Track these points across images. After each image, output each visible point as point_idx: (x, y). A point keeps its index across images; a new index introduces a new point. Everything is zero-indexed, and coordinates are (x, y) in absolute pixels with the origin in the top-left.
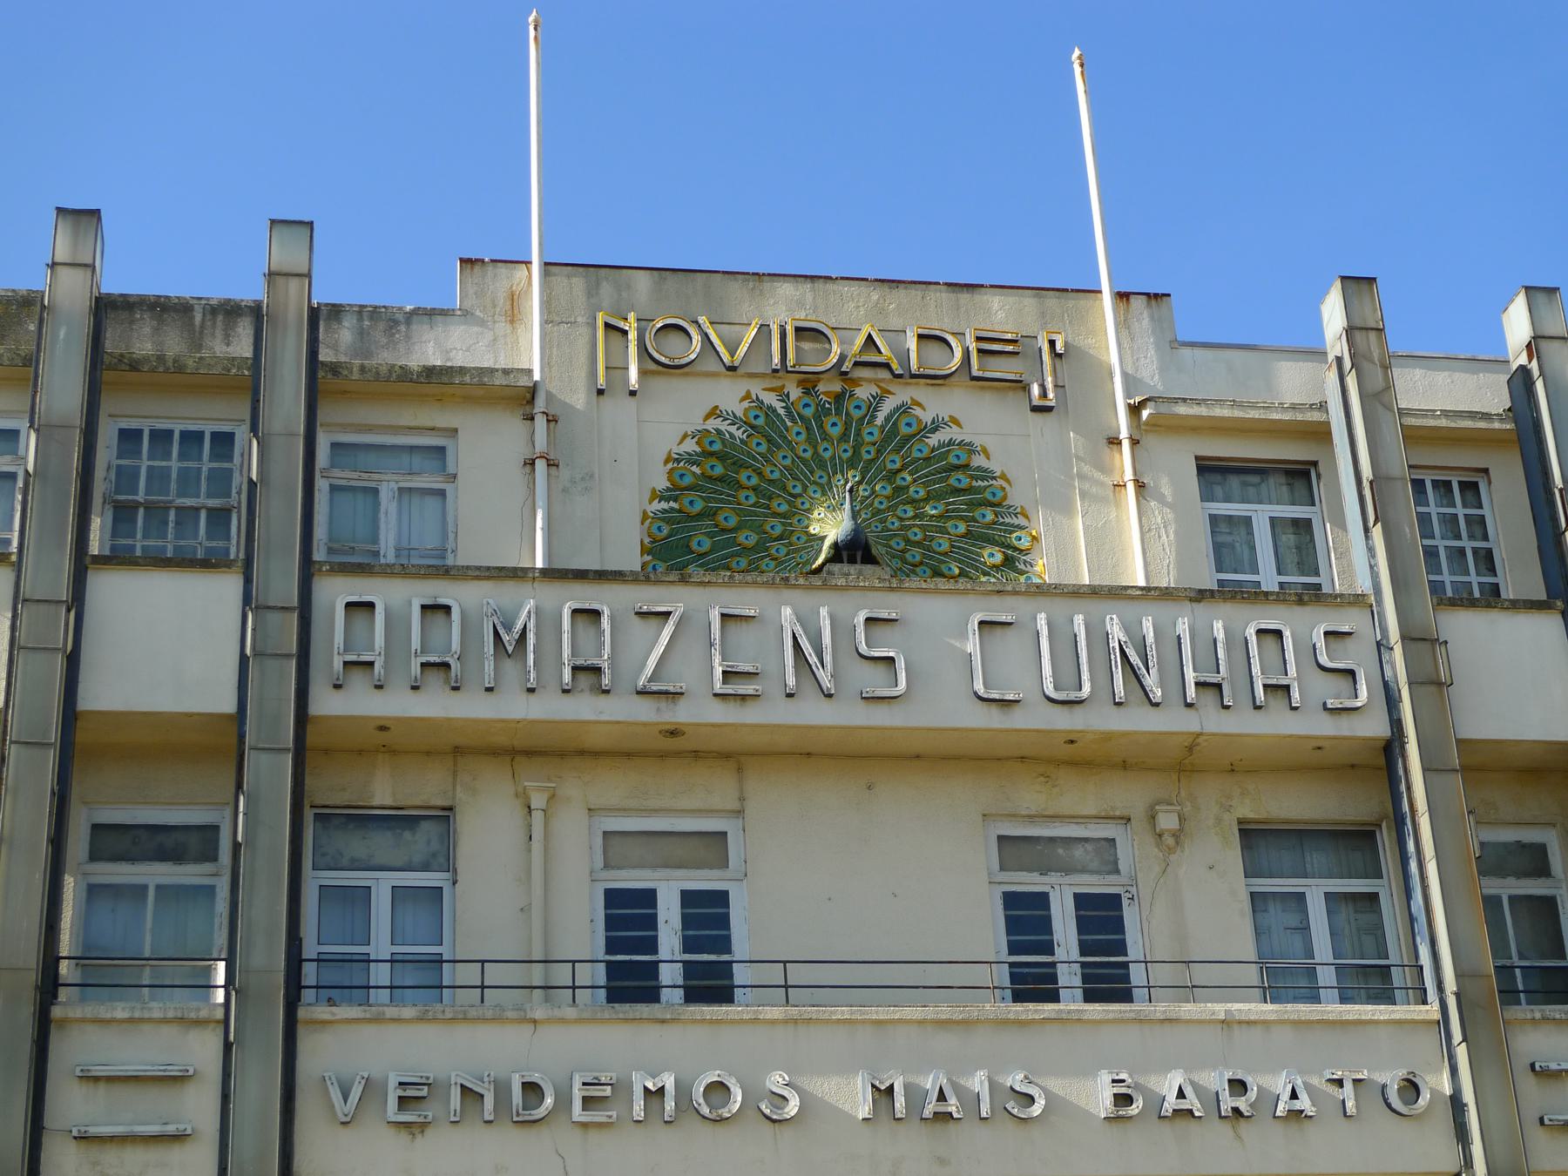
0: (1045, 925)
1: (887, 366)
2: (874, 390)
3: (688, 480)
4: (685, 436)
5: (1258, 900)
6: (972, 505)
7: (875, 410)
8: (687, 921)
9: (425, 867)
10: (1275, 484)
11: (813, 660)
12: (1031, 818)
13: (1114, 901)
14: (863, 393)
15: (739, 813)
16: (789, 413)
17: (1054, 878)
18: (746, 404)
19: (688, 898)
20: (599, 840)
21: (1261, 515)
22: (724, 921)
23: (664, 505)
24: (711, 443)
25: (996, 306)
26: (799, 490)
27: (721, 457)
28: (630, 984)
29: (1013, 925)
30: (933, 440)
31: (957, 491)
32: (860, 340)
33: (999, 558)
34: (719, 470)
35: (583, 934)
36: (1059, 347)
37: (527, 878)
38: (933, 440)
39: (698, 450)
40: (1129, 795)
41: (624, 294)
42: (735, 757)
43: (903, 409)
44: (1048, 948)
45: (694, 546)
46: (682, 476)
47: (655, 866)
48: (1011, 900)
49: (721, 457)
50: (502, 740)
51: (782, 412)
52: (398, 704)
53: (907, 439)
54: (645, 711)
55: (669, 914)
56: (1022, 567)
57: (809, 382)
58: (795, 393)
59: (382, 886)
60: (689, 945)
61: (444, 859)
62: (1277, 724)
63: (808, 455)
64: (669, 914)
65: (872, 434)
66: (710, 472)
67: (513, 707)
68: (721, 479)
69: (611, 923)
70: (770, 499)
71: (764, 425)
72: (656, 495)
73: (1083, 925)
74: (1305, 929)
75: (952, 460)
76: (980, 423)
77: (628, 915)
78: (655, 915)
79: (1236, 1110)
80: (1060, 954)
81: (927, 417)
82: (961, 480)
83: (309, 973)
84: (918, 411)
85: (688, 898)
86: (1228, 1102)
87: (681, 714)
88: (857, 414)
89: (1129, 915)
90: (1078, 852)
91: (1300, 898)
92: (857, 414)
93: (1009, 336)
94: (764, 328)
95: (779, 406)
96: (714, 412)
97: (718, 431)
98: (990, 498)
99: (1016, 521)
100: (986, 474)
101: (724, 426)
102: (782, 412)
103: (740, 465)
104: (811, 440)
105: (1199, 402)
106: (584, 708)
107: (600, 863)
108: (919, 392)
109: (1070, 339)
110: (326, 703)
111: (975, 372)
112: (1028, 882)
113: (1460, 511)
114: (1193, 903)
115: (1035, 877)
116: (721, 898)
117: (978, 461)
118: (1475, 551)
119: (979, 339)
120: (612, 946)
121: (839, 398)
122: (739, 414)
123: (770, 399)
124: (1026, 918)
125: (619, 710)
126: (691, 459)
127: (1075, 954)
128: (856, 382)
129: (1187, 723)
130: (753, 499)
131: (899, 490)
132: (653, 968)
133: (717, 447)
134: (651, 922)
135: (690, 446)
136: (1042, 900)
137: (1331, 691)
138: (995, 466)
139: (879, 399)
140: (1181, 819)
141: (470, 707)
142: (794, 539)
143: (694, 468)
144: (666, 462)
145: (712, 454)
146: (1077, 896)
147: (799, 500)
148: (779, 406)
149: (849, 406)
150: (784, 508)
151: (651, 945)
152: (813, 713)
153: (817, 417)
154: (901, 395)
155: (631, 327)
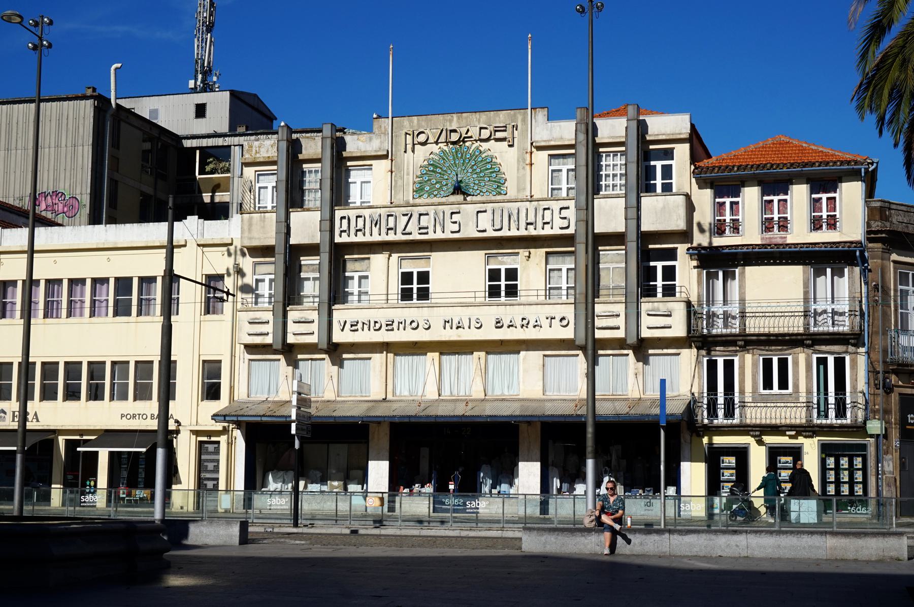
14: (467, 144)
31: (487, 169)
32: (464, 130)
35: (396, 286)
52: (353, 239)
57: (454, 143)
62: (548, 231)
67: (376, 238)
71: (443, 155)
72: (417, 177)
76: (496, 149)
77: (406, 278)
82: (489, 166)
91: (560, 270)
100: (496, 164)
103: (437, 167)
104: (454, 159)
106: (391, 237)
108: (482, 144)
117: (494, 160)
123: (446, 148)
125: (400, 237)
131: (474, 170)
135: (426, 163)
138: (498, 161)
141: (367, 239)
152: (440, 235)
153: (456, 152)
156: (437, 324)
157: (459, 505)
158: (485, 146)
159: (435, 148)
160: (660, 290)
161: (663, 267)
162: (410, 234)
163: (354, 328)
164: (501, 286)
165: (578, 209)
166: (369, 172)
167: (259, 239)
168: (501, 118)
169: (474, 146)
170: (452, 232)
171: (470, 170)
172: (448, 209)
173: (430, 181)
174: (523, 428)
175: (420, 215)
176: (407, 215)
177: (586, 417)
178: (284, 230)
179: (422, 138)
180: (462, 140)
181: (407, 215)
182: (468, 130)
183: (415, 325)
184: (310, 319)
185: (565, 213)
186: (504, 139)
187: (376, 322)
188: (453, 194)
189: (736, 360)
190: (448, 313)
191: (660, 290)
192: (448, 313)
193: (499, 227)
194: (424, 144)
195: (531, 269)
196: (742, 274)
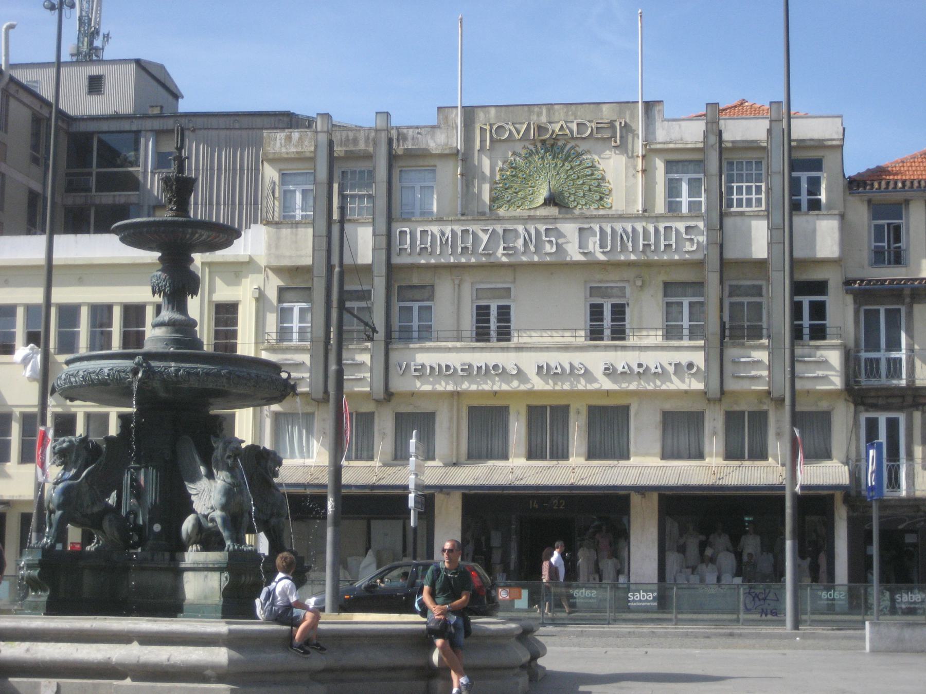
0: (602, 313)
2: (564, 142)
5: (668, 304)
8: (499, 314)
9: (428, 300)
10: (691, 167)
12: (600, 282)
13: (623, 306)
14: (560, 143)
15: (514, 282)
19: (499, 307)
20: (475, 292)
21: (685, 177)
22: (509, 314)
27: (515, 168)
28: (482, 335)
29: (592, 313)
32: (557, 127)
35: (468, 321)
37: (451, 305)
40: (629, 274)
42: (513, 267)
43: (573, 148)
44: (602, 320)
47: (490, 299)
48: (592, 306)
49: (515, 168)
55: (494, 312)
59: (416, 306)
60: (499, 321)
61: (431, 298)
64: (494, 312)
68: (514, 176)
69: (478, 315)
73: (613, 313)
74: (682, 312)
77: (482, 313)
79: (639, 372)
81: (579, 150)
83: (395, 335)
84: (577, 149)
85: (499, 307)
86: (636, 369)
88: (557, 151)
89: (627, 310)
91: (682, 303)
92: (557, 151)
94: (529, 125)
107: (475, 297)
108: (579, 143)
109: (628, 121)
112: (598, 301)
114: (647, 308)
116: (508, 307)
120: (478, 321)
121: (552, 146)
124: (596, 312)
128: (558, 140)
134: (489, 314)
139: (565, 145)
140: (643, 281)
149: (555, 148)
151: (488, 321)
155: (488, 127)
157: (591, 598)
158: (582, 147)
160: (806, 331)
161: (811, 303)
165: (709, 228)
167: (291, 257)
174: (635, 499)
177: (782, 488)
178: (324, 247)
187: (448, 367)
189: (902, 418)
190: (544, 358)
191: (806, 331)
192: (544, 358)
196: (910, 314)
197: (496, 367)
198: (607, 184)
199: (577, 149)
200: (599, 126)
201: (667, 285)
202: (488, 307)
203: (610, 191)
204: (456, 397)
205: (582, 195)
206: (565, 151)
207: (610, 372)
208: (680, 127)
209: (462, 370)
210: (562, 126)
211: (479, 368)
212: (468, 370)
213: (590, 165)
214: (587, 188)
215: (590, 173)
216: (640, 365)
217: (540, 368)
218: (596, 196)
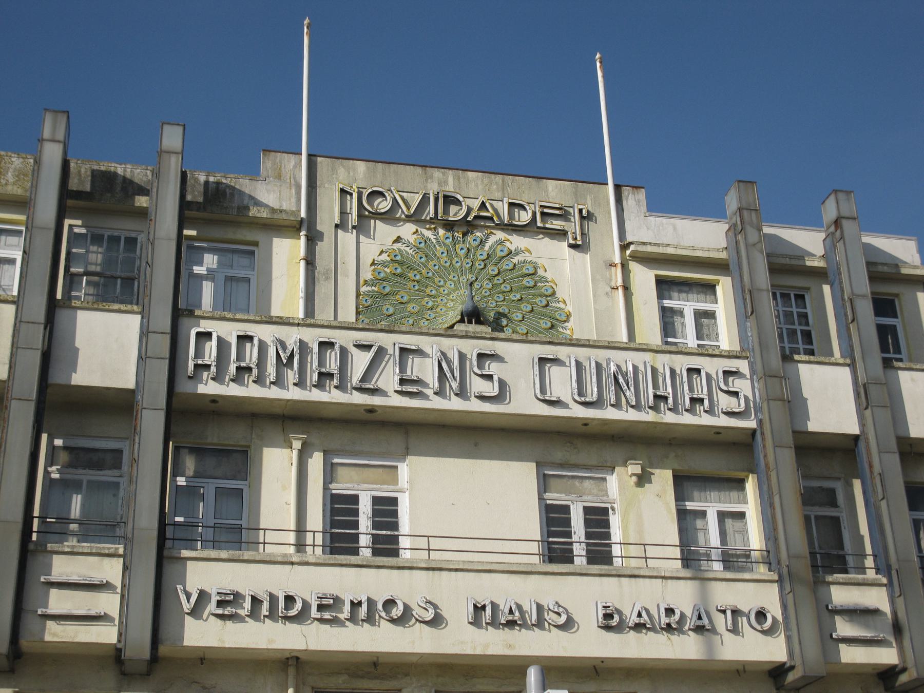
0: (567, 522)
1: (491, 219)
3: (382, 275)
4: (382, 252)
6: (534, 295)
7: (485, 242)
8: (375, 513)
9: (234, 478)
11: (449, 375)
13: (605, 511)
16: (438, 242)
17: (574, 497)
18: (415, 236)
19: (376, 500)
22: (395, 514)
23: (369, 288)
24: (396, 256)
25: (550, 189)
26: (442, 283)
27: (401, 263)
30: (515, 260)
32: (476, 204)
33: (549, 325)
34: (399, 271)
36: (584, 213)
38: (515, 260)
39: (388, 259)
41: (351, 174)
43: (501, 242)
45: (385, 312)
46: (379, 273)
49: (401, 263)
50: (278, 411)
51: (434, 241)
53: (501, 259)
54: (358, 398)
55: (365, 507)
56: (561, 330)
58: (441, 232)
60: (376, 525)
63: (448, 264)
64: (365, 507)
65: (482, 254)
66: (394, 272)
68: (400, 275)
70: (426, 287)
71: (424, 247)
73: (588, 523)
75: (525, 271)
78: (358, 509)
80: (575, 538)
84: (508, 244)
86: (664, 620)
87: (376, 401)
90: (587, 484)
93: (557, 206)
95: (432, 237)
96: (398, 240)
97: (399, 249)
98: (546, 293)
99: (558, 305)
100: (544, 280)
101: (403, 247)
102: (434, 241)
103: (411, 268)
105: (659, 245)
109: (590, 209)
110: (184, 387)
111: (539, 224)
113: (795, 310)
115: (563, 496)
116: (394, 501)
117: (541, 272)
118: (802, 331)
119: (541, 206)
122: (412, 241)
126: (385, 264)
127: (583, 539)
129: (649, 416)
130: (417, 288)
132: (355, 538)
133: (398, 258)
134: (356, 513)
135: (385, 257)
136: (566, 509)
137: (725, 402)
138: (549, 275)
142: (438, 310)
143: (388, 270)
144: (371, 265)
145: (396, 262)
146: (585, 508)
147: (442, 289)
148: (432, 237)
150: (434, 292)
151: (355, 525)
154: (500, 235)
156: (458, 614)
158: (517, 242)
159: (407, 231)
162: (374, 391)
163: (220, 611)
164: (571, 540)
166: (245, 261)
168: (555, 192)
169: (492, 240)
170: (482, 398)
171: (487, 285)
172: (471, 348)
173: (388, 300)
175: (403, 350)
176: (368, 347)
179: (384, 205)
180: (468, 225)
181: (368, 347)
182: (483, 206)
183: (397, 612)
184: (97, 576)
185: (738, 384)
186: (561, 234)
187: (290, 599)
188: (462, 321)
193: (595, 397)
194: (388, 217)
195: (641, 508)
197: (389, 603)
198: (561, 305)
199: (508, 244)
200: (546, 210)
201: (679, 480)
202: (355, 499)
203: (568, 316)
204: (292, 671)
205: (520, 317)
206: (487, 246)
207: (611, 621)
208: (675, 229)
209: (321, 608)
210: (483, 204)
211: (355, 605)
212: (329, 607)
213: (532, 271)
214: (529, 308)
215: (532, 284)
216: (670, 611)
217: (479, 609)
218: (545, 324)
